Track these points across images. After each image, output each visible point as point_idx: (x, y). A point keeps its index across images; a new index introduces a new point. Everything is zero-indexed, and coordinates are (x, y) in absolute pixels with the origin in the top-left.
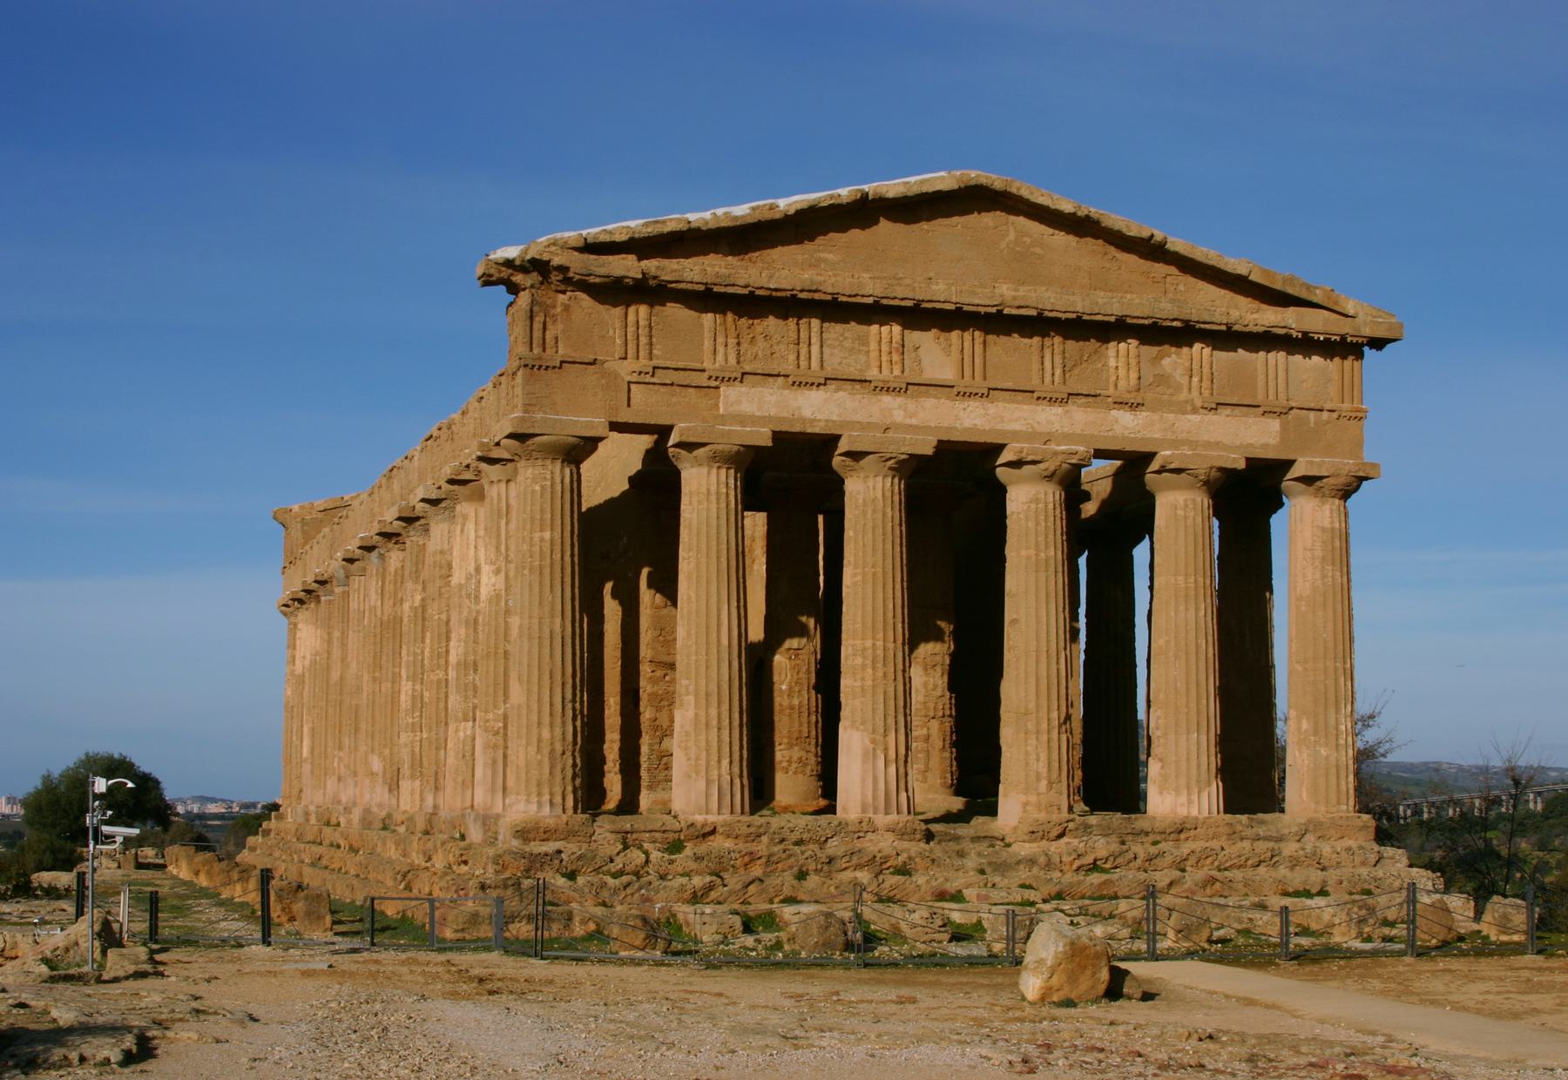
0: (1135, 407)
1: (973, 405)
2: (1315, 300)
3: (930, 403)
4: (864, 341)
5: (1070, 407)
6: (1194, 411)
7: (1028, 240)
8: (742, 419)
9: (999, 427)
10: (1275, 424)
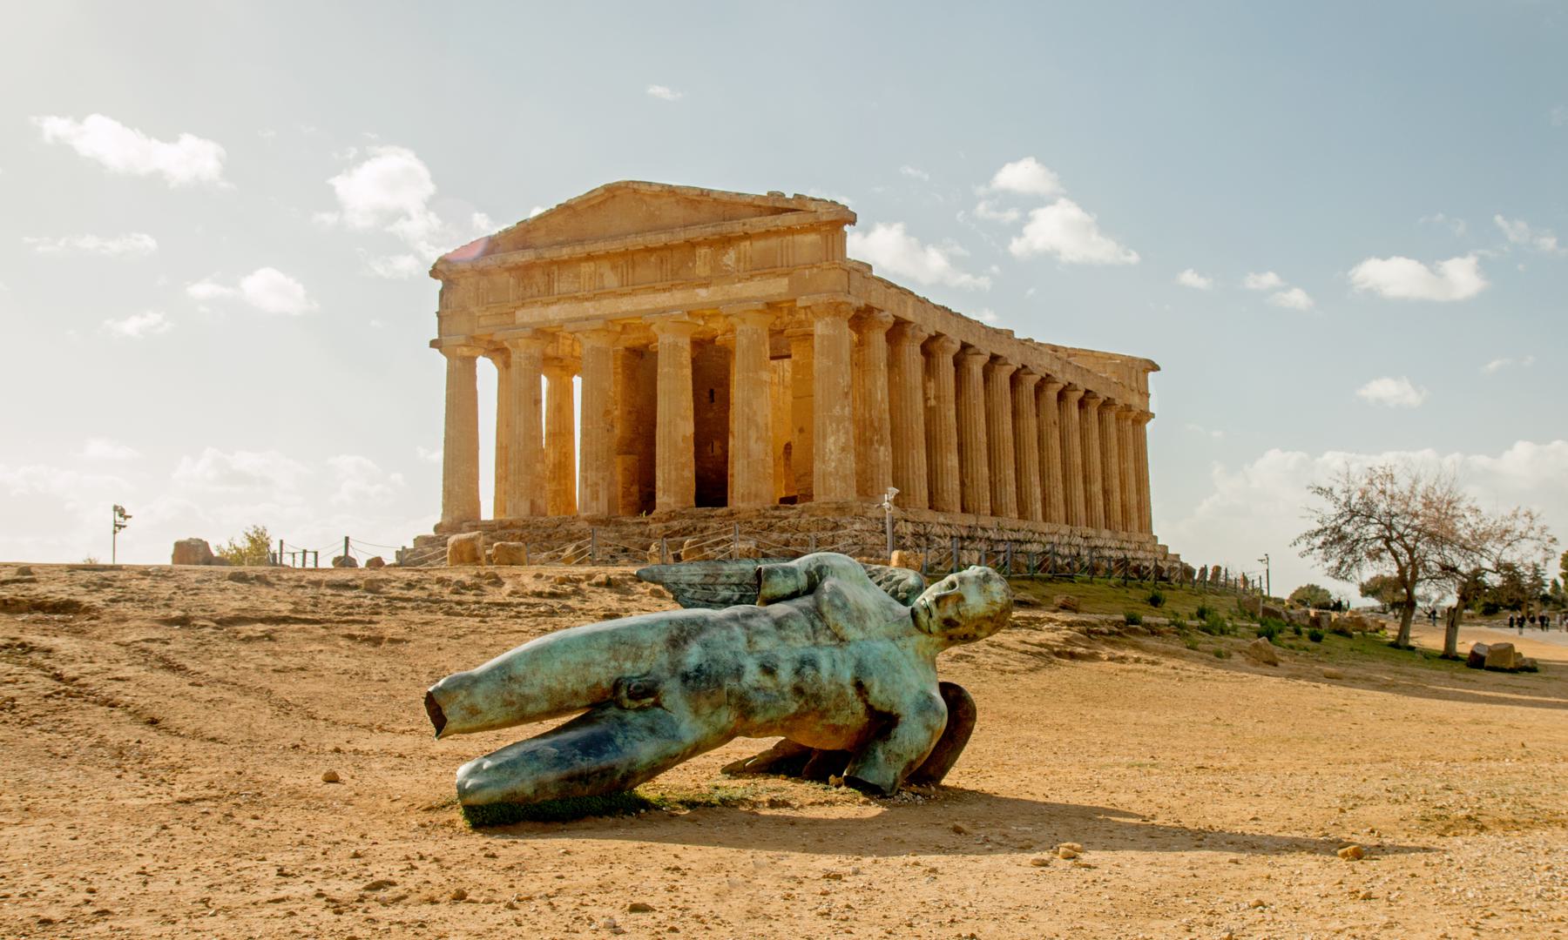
0: (707, 286)
1: (625, 300)
2: (791, 207)
3: (605, 302)
4: (578, 276)
5: (675, 292)
6: (739, 281)
7: (652, 209)
8: (524, 326)
9: (639, 308)
10: (785, 281)
